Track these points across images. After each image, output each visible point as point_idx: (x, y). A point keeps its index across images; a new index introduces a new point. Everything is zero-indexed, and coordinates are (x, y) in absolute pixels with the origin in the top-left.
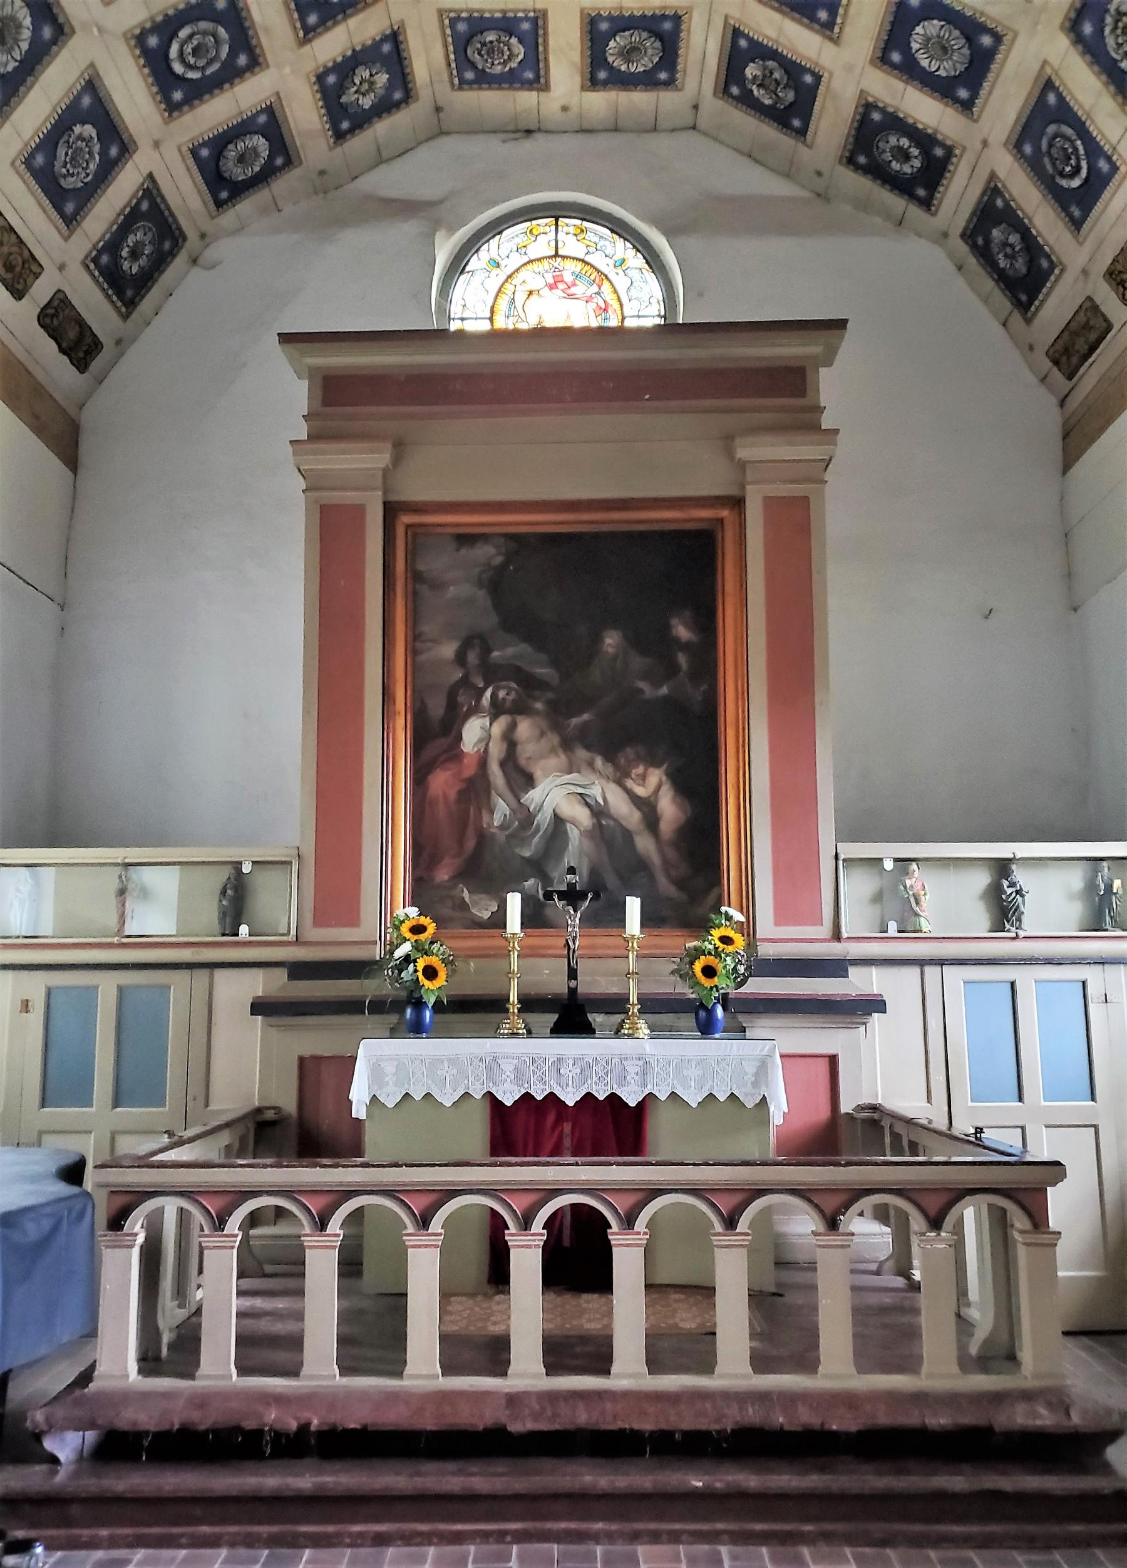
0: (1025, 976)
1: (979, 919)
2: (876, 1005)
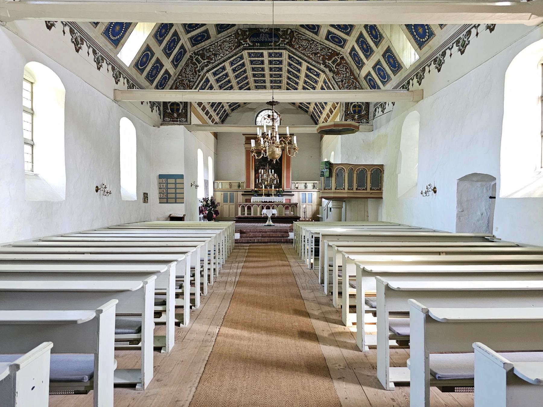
0: (307, 193)
1: (304, 188)
2: (294, 195)
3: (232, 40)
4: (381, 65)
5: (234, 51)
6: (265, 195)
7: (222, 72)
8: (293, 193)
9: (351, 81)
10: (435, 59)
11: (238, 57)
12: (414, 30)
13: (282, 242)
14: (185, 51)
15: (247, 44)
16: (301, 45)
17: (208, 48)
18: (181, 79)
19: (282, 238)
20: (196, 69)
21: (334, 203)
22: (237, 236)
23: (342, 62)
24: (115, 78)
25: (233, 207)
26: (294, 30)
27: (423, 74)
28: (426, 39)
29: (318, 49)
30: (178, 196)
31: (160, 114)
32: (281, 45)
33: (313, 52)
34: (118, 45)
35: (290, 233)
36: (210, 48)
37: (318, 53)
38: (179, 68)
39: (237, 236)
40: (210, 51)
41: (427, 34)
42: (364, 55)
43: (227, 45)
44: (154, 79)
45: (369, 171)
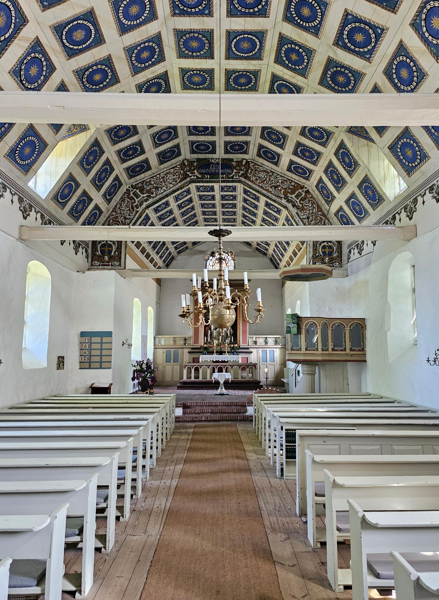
0: (268, 350)
2: (252, 352)
3: (177, 172)
4: (356, 198)
5: (179, 184)
6: (217, 352)
7: (165, 208)
8: (251, 350)
9: (318, 218)
10: (430, 187)
11: (184, 192)
12: (400, 154)
13: (238, 420)
14: (121, 184)
15: (194, 176)
16: (259, 177)
17: (149, 180)
18: (115, 216)
19: (238, 414)
20: (134, 205)
21: (305, 368)
22: (179, 412)
23: (307, 196)
24: (23, 212)
25: (177, 367)
26: (249, 160)
27: (415, 206)
28: (416, 163)
29: (278, 182)
30: (104, 359)
31: (87, 257)
32: (235, 177)
33: (272, 185)
34: (28, 171)
35: (248, 408)
36: (150, 181)
37: (279, 186)
38: (113, 203)
39: (179, 412)
40: (151, 184)
41: (419, 157)
42: (335, 187)
43: (170, 177)
44: (80, 216)
45: (347, 326)
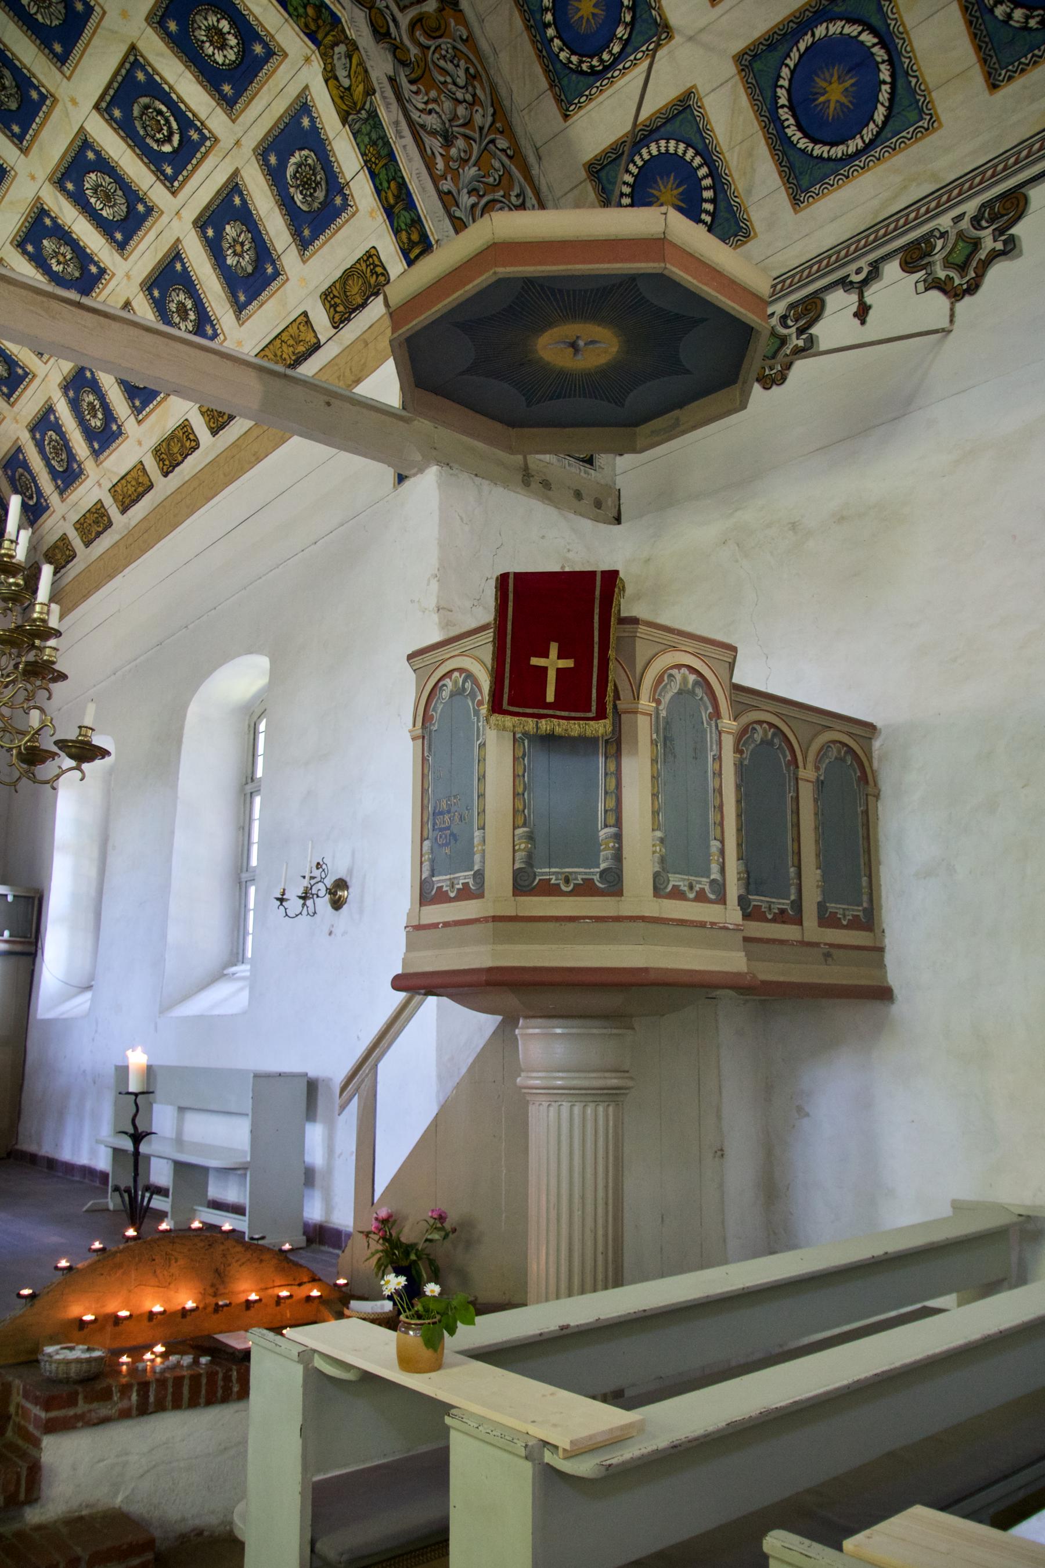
9: (497, 164)
